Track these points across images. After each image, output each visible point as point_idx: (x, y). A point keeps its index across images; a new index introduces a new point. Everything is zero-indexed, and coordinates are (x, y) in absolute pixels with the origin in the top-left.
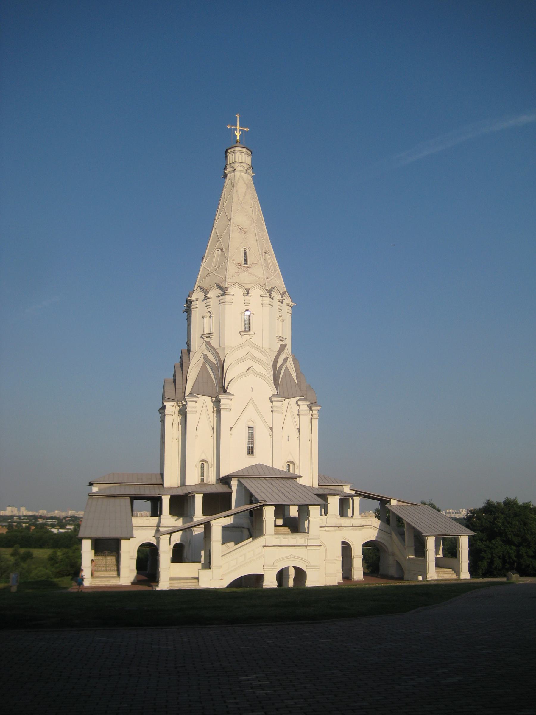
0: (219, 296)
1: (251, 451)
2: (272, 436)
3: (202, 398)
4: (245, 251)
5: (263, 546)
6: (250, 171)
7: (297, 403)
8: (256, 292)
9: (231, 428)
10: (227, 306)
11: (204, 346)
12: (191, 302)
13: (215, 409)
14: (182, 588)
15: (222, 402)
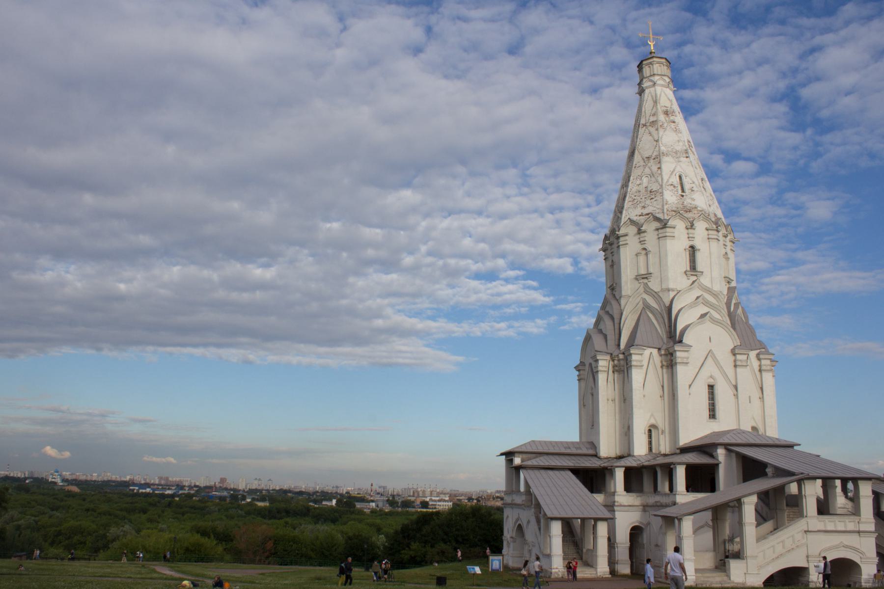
0: (657, 229)
1: (713, 415)
2: (736, 396)
3: (648, 352)
4: (680, 177)
5: (806, 532)
6: (671, 86)
7: (758, 355)
8: (701, 226)
9: (690, 386)
10: (669, 242)
11: (642, 290)
12: (618, 238)
13: (665, 363)
15: (678, 354)
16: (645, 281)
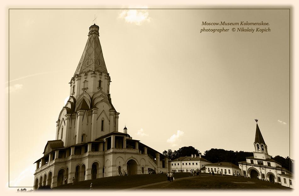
1: (102, 130)
2: (109, 124)
16: (85, 90)
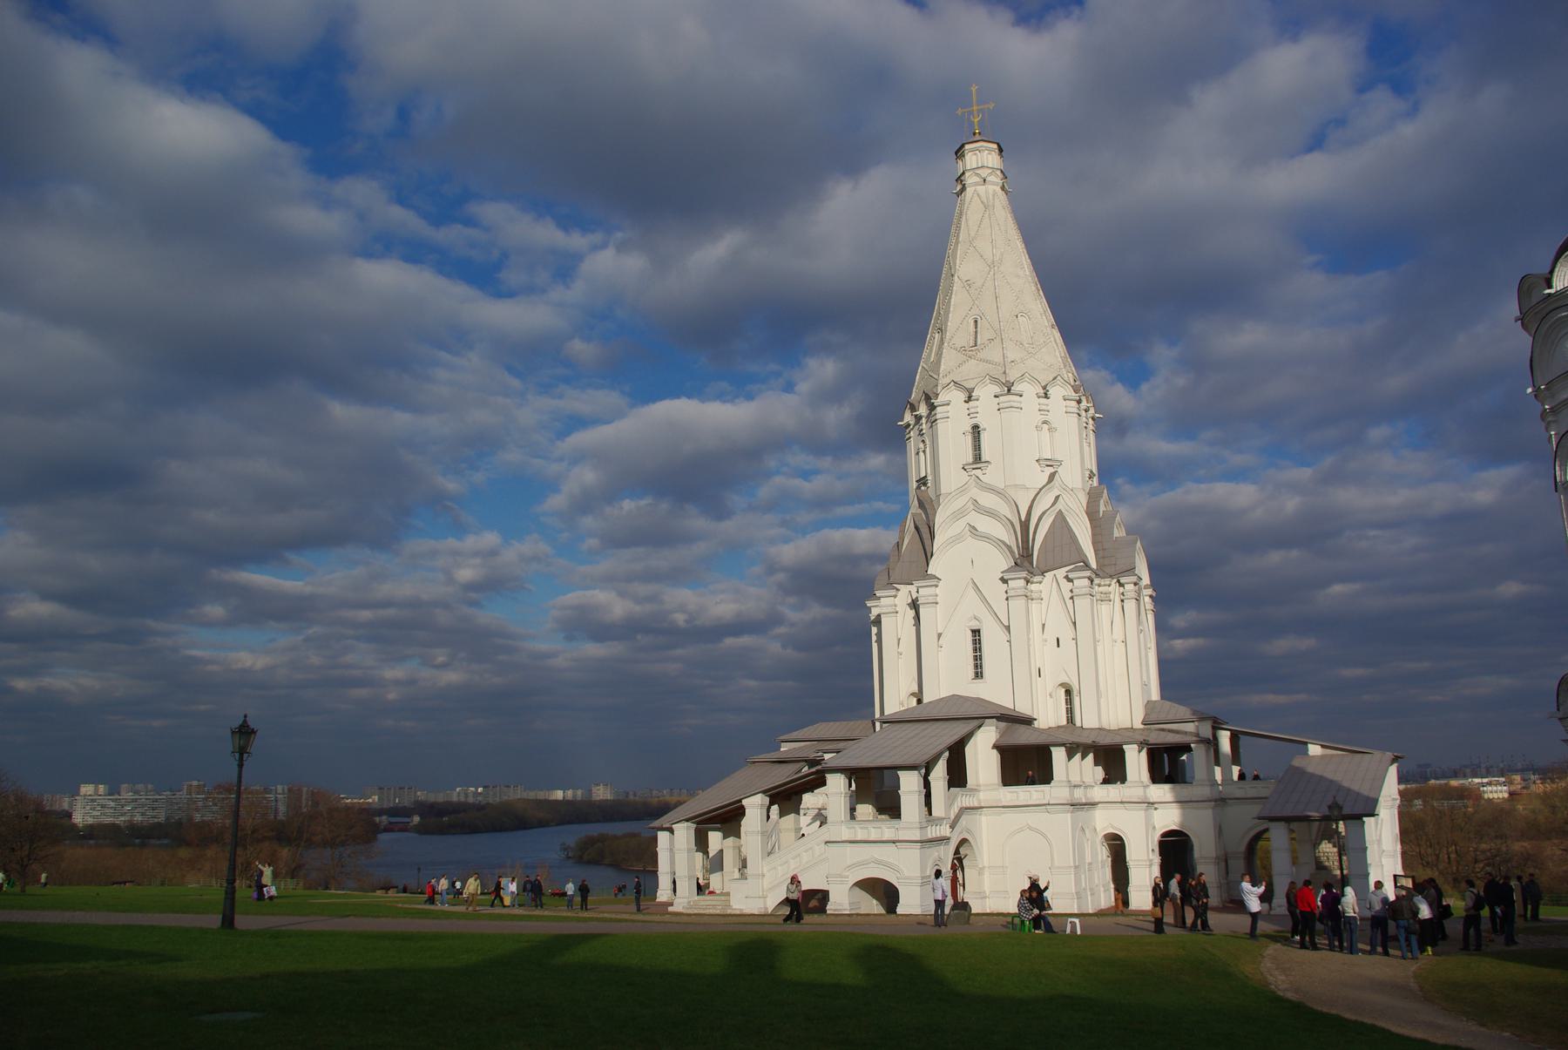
1: (979, 675)
8: (986, 392)
9: (939, 635)
14: (748, 911)
